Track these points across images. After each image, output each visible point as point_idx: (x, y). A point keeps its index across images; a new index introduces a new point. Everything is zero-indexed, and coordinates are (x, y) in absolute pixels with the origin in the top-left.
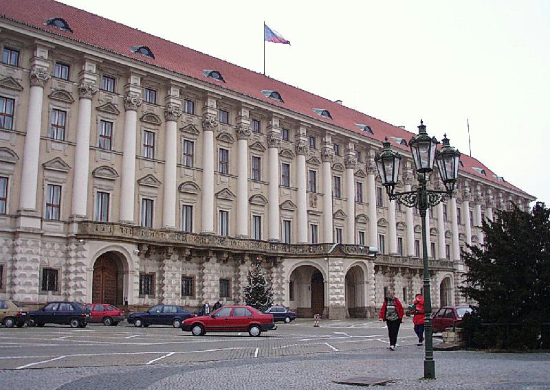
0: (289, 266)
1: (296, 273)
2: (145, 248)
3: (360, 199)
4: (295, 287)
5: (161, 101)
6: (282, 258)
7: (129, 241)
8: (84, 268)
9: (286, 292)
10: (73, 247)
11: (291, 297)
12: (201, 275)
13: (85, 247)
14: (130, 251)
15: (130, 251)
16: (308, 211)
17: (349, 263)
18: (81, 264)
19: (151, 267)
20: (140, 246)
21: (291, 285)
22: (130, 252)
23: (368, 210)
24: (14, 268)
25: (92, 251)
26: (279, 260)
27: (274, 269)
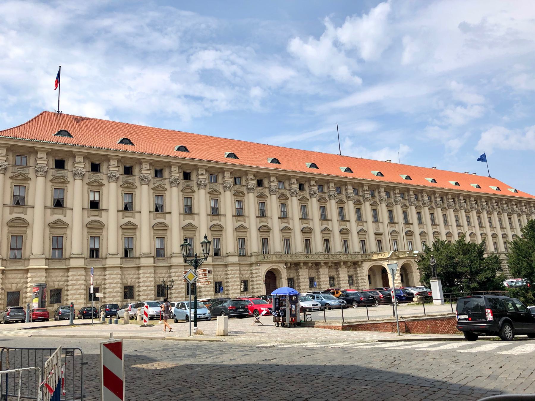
0: (366, 266)
1: (371, 269)
2: (289, 265)
3: (406, 222)
4: (372, 277)
5: (287, 187)
6: (362, 262)
7: (279, 262)
8: (260, 278)
9: (367, 280)
10: (254, 268)
11: (370, 283)
12: (319, 275)
13: (260, 267)
14: (282, 268)
15: (282, 268)
16: (375, 233)
17: (402, 262)
18: (259, 276)
19: (293, 275)
20: (286, 264)
21: (369, 276)
22: (282, 267)
23: (413, 228)
24: (227, 282)
25: (264, 269)
26: (360, 263)
27: (358, 269)
